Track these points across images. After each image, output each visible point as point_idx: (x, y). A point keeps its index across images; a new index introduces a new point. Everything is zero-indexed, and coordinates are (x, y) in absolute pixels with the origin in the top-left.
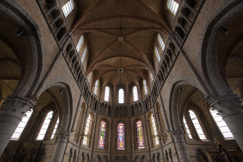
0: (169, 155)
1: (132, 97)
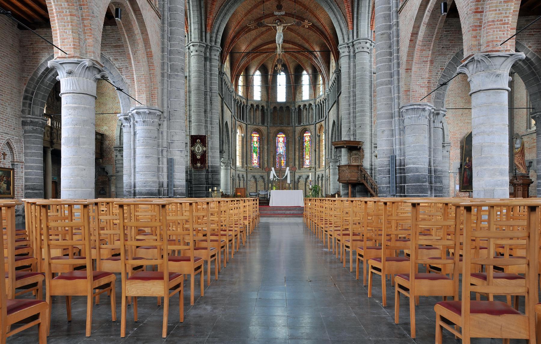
0: (320, 179)
1: (301, 92)
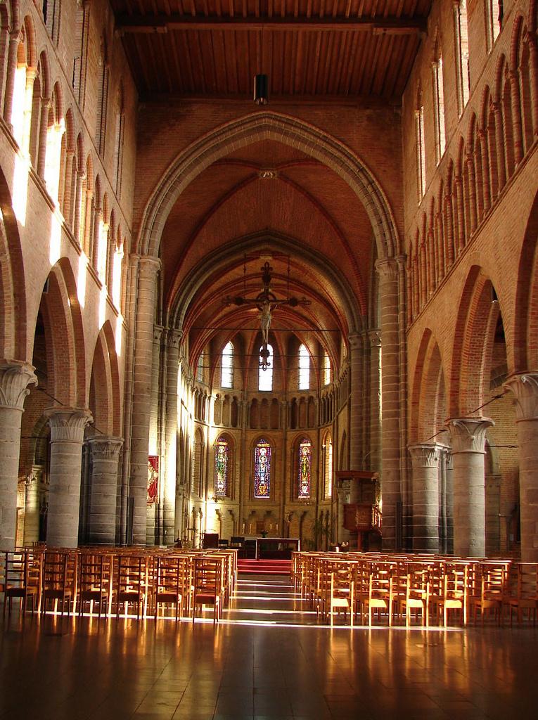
0: (324, 517)
1: (297, 377)
